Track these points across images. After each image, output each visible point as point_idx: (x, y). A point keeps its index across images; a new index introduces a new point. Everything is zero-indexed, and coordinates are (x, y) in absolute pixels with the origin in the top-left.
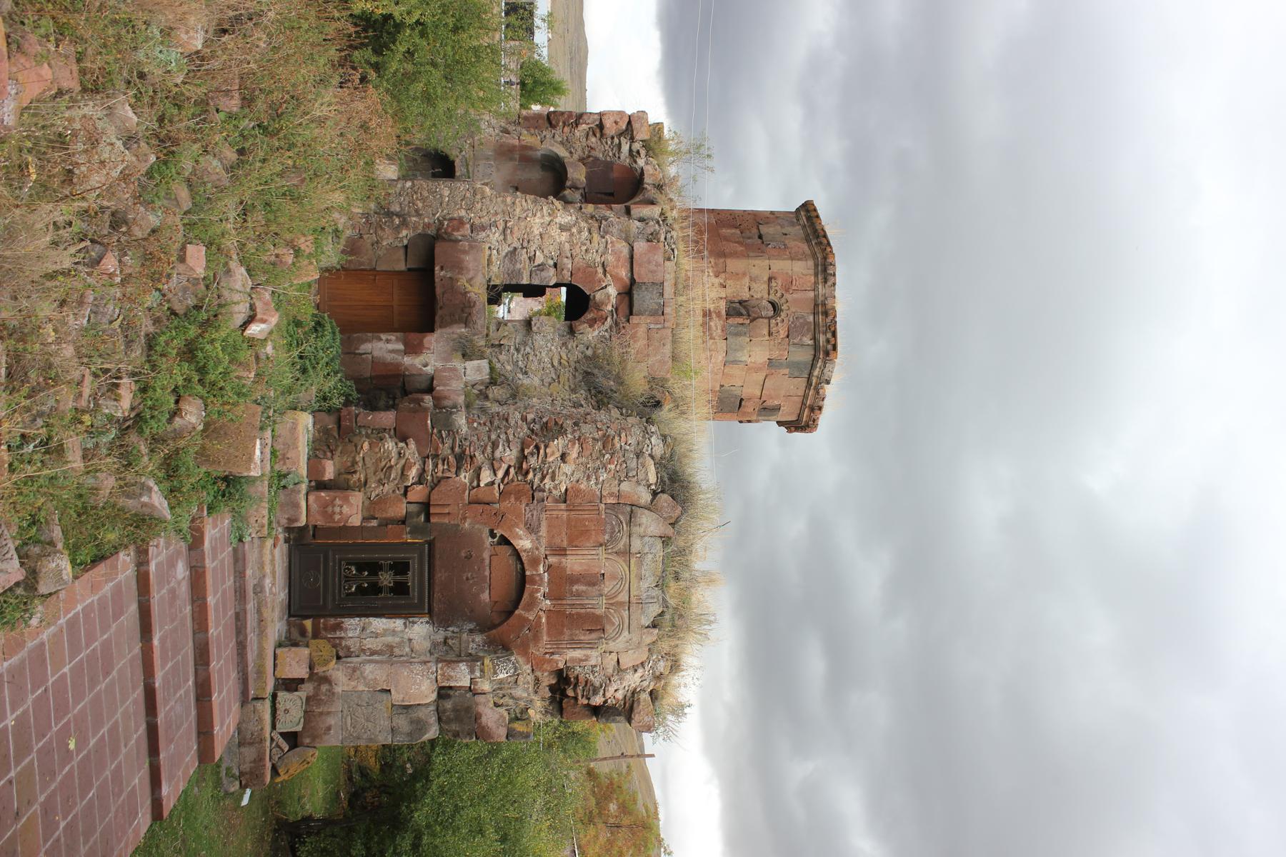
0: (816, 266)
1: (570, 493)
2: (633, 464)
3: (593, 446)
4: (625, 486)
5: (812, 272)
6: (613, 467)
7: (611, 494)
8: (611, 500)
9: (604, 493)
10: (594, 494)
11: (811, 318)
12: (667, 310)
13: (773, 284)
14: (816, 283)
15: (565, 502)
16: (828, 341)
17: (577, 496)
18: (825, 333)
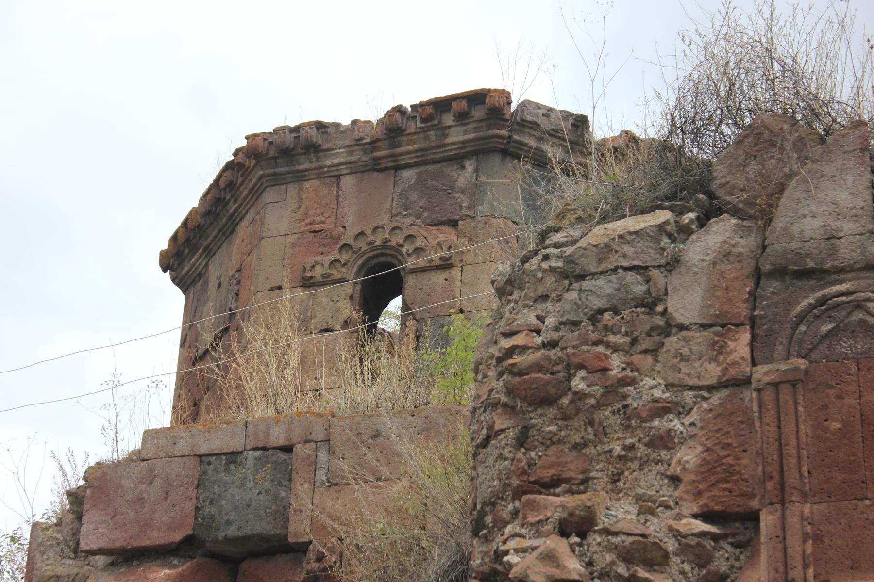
0: (277, 180)
1: (718, 498)
2: (602, 289)
3: (551, 441)
4: (686, 302)
5: (292, 189)
6: (616, 361)
7: (718, 349)
8: (740, 345)
9: (712, 372)
10: (721, 414)
11: (409, 175)
12: (278, 437)
13: (318, 272)
14: (320, 174)
15: (753, 518)
16: (462, 117)
17: (730, 473)
18: (443, 130)
